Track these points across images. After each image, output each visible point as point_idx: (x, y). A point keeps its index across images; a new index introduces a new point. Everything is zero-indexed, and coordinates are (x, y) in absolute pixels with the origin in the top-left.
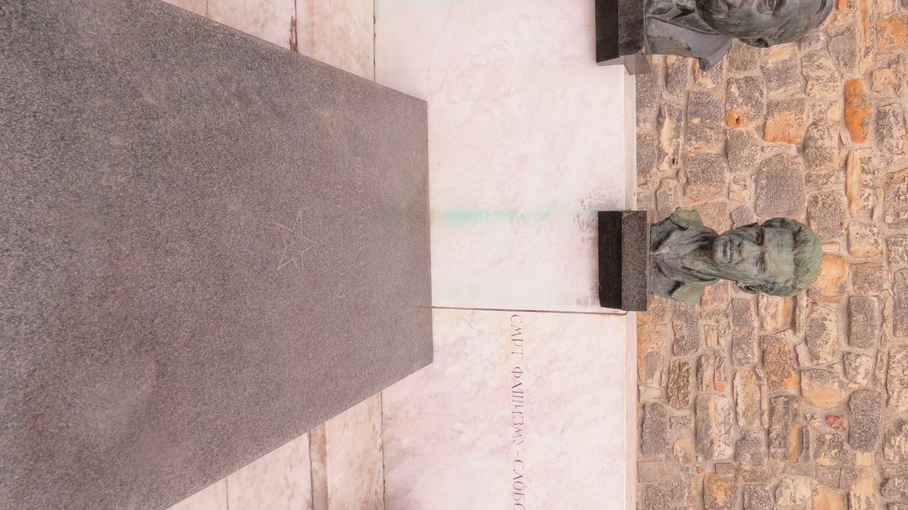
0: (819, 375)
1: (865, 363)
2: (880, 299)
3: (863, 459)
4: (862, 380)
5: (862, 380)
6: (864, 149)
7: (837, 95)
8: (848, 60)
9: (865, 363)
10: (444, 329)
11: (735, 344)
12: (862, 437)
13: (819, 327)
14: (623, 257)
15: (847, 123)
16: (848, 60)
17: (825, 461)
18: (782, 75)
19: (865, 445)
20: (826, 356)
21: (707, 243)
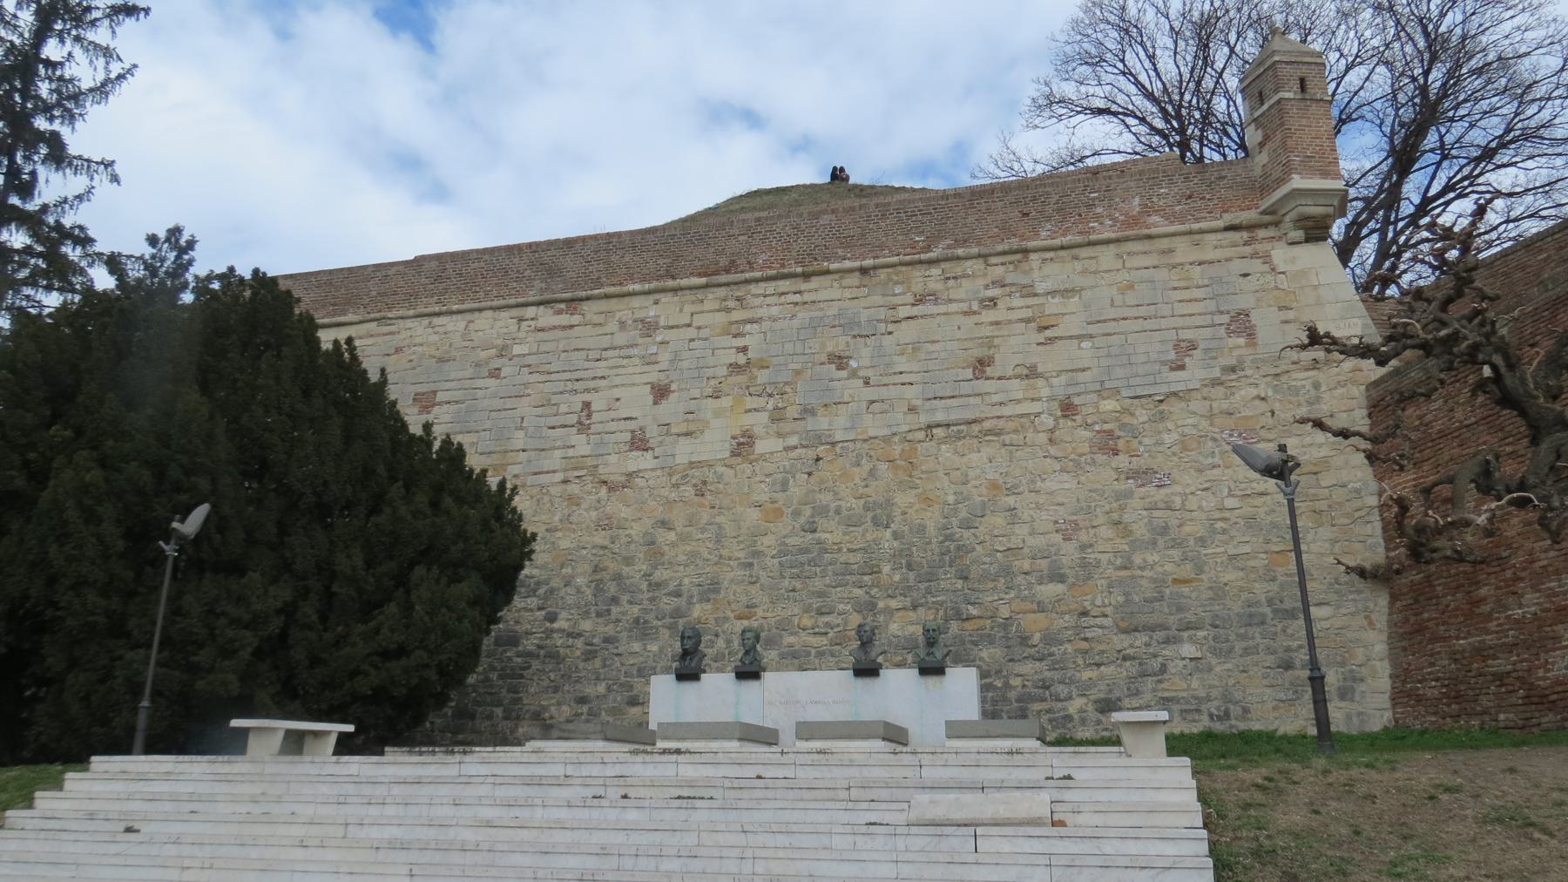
0: (846, 624)
1: (841, 607)
2: (816, 603)
3: (881, 605)
4: (849, 607)
5: (849, 607)
6: (760, 613)
7: (738, 623)
8: (726, 619)
9: (841, 607)
10: (769, 724)
11: (832, 655)
12: (871, 606)
13: (827, 624)
14: (749, 672)
15: (748, 618)
16: (726, 619)
17: (881, 618)
18: (728, 642)
19: (874, 605)
20: (839, 621)
21: (747, 653)
